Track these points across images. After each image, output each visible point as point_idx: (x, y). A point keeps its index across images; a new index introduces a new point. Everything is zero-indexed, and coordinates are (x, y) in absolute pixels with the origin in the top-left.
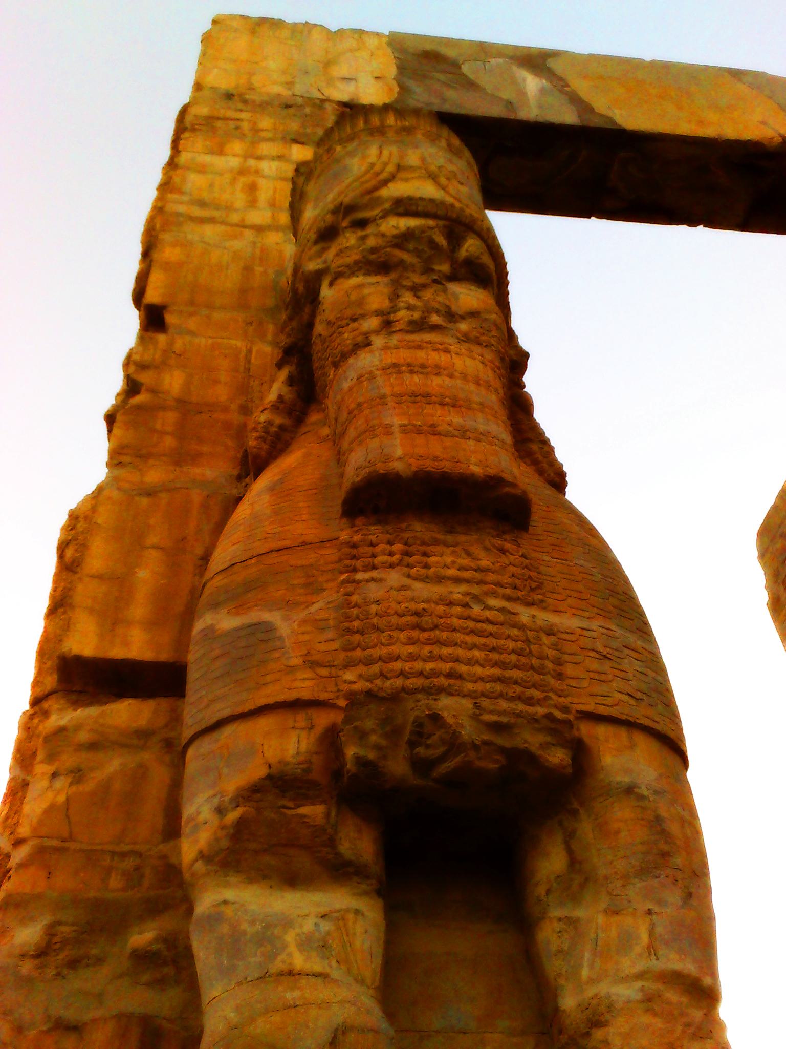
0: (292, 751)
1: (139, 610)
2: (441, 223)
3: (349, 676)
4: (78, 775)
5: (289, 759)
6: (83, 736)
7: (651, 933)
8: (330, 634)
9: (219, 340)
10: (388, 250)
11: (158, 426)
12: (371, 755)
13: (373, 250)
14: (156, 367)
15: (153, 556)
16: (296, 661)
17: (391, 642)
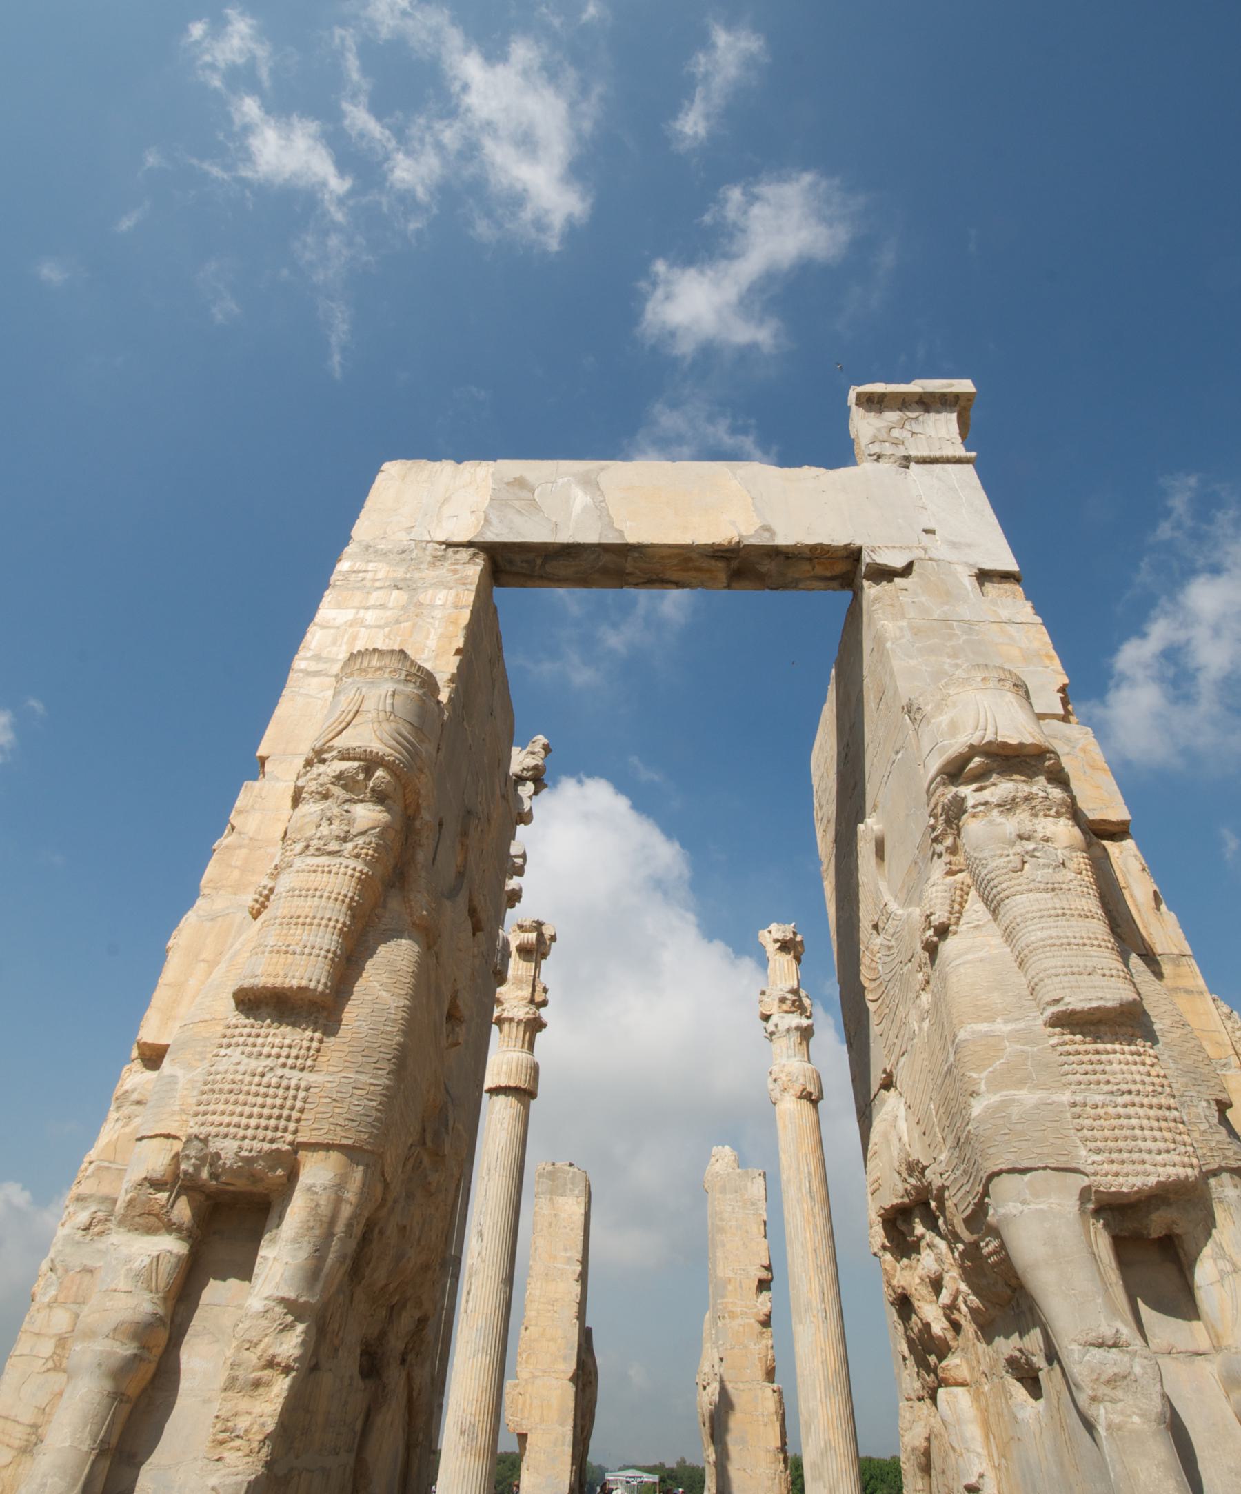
5: (157, 1168)
8: (195, 1093)
12: (191, 1170)
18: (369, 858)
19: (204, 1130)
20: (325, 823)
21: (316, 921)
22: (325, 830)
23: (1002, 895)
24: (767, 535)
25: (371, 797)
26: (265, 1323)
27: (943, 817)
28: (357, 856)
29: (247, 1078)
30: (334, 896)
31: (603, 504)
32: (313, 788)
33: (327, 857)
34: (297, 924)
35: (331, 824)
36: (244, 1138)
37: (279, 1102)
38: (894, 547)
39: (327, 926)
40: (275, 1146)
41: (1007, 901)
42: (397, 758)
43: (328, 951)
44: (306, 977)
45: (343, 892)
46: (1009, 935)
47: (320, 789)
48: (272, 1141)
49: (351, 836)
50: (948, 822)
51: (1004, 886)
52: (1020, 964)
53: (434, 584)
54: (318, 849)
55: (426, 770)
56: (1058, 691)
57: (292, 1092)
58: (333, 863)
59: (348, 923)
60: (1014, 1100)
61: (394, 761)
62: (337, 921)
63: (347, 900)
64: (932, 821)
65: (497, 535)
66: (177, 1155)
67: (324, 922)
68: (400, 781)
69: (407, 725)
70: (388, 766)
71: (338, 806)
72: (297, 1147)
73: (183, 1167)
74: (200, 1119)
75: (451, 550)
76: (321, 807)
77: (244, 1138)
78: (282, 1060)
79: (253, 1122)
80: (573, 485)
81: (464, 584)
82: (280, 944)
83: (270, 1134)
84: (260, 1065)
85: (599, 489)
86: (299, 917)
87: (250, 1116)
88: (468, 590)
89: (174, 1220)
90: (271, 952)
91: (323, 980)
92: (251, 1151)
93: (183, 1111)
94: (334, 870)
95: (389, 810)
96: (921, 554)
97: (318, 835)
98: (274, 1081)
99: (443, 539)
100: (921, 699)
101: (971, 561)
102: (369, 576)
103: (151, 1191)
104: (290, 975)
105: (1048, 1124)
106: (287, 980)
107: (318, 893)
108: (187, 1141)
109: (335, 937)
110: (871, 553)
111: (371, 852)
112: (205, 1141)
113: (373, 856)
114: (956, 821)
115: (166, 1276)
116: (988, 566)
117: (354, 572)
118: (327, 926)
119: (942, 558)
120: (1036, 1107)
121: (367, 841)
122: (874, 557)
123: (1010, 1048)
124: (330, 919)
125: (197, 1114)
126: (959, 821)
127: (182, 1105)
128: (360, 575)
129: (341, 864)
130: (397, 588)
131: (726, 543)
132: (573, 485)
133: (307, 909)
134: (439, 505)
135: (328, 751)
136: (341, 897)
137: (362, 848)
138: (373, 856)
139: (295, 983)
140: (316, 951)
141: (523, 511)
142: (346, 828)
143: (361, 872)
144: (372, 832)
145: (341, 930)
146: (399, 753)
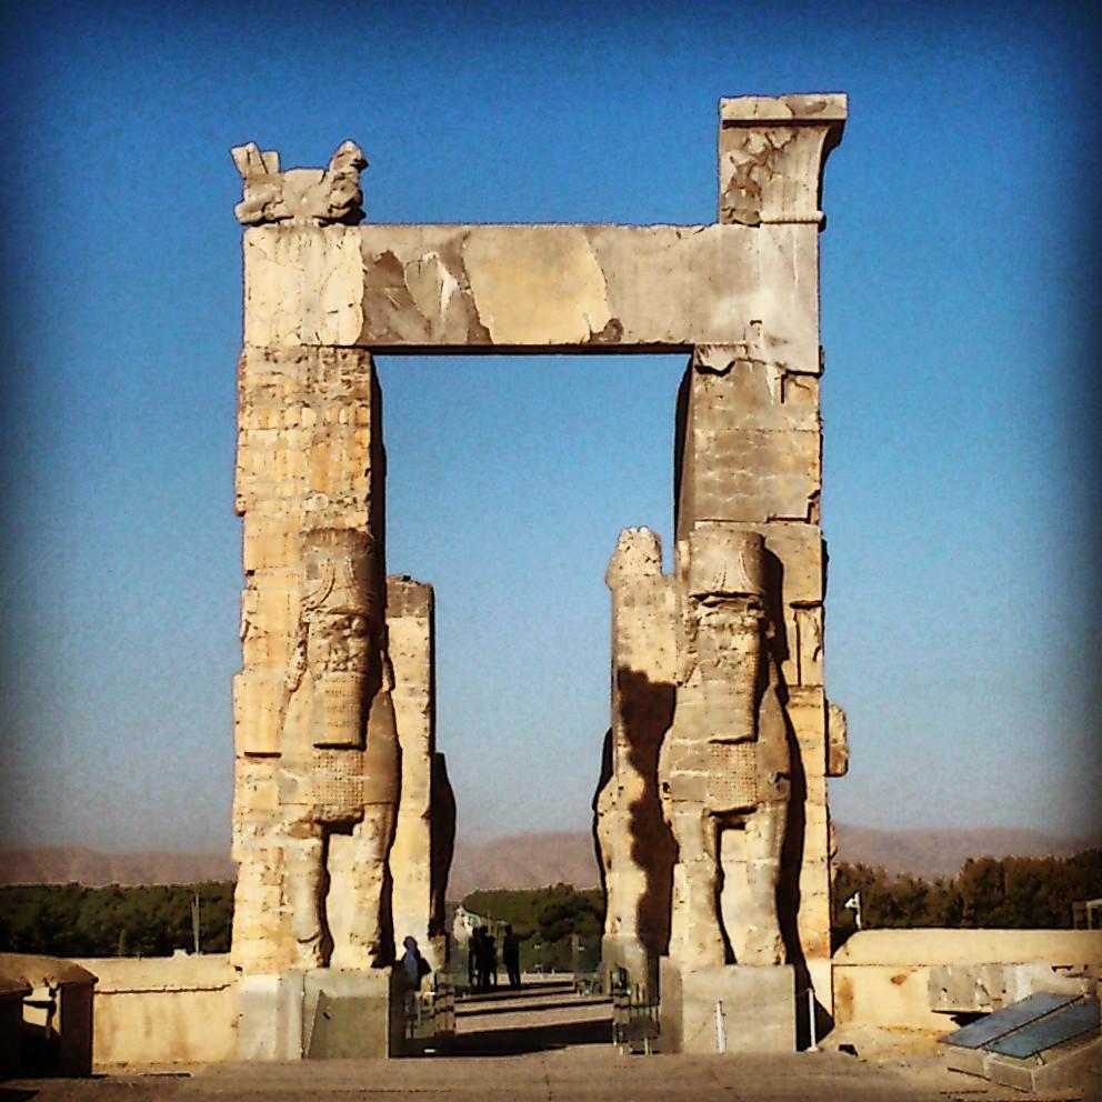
1: (264, 734)
22: (334, 657)
24: (615, 331)
31: (468, 291)
38: (721, 346)
50: (692, 625)
53: (334, 399)
65: (379, 337)
72: (363, 806)
75: (339, 351)
80: (439, 263)
81: (360, 399)
84: (339, 775)
85: (464, 271)
88: (363, 406)
96: (742, 353)
99: (331, 343)
101: (782, 362)
102: (277, 391)
110: (701, 354)
116: (792, 368)
117: (264, 387)
119: (758, 358)
122: (703, 358)
123: (689, 752)
128: (271, 390)
130: (307, 406)
131: (578, 342)
132: (439, 263)
134: (317, 294)
135: (325, 607)
141: (398, 304)
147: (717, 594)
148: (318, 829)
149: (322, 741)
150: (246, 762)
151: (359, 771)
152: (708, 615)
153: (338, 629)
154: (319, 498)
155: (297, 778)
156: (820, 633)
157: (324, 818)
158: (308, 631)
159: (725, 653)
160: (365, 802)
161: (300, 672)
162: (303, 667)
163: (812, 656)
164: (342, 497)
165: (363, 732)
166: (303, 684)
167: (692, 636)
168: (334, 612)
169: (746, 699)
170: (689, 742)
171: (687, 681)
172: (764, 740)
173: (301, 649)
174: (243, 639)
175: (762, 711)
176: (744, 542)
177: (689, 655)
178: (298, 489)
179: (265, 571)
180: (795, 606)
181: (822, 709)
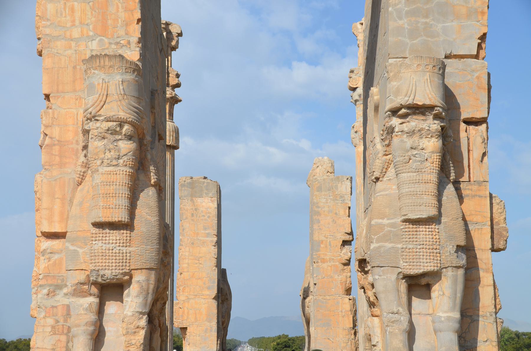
0: (82, 278)
1: (56, 218)
2: (117, 123)
3: (91, 266)
4: (49, 259)
6: (49, 251)
7: (136, 306)
8: (88, 256)
9: (68, 110)
10: (103, 134)
11: (54, 153)
12: (95, 279)
13: (101, 133)
14: (51, 126)
15: (58, 200)
16: (82, 261)
17: (98, 259)
18: (131, 165)
19: (97, 268)
20: (107, 152)
21: (117, 195)
22: (108, 155)
23: (398, 172)
25: (125, 138)
26: (134, 318)
27: (386, 132)
28: (126, 166)
29: (107, 251)
30: (121, 184)
32: (96, 134)
33: (113, 167)
34: (109, 197)
35: (110, 152)
36: (112, 270)
37: (121, 258)
39: (122, 196)
40: (124, 271)
41: (399, 175)
42: (133, 119)
43: (125, 206)
44: (120, 217)
45: (124, 182)
46: (398, 187)
47: (100, 135)
48: (122, 270)
49: (121, 157)
51: (400, 169)
52: (399, 198)
54: (109, 164)
55: (145, 117)
56: (479, 39)
57: (125, 255)
58: (117, 170)
59: (129, 194)
60: (383, 246)
61: (132, 121)
62: (125, 194)
63: (127, 185)
64: (382, 132)
66: (88, 275)
67: (120, 195)
68: (135, 128)
69: (133, 98)
70: (131, 123)
71: (111, 143)
73: (91, 279)
74: (93, 264)
76: (103, 143)
77: (112, 270)
78: (118, 244)
79: (114, 265)
82: (105, 205)
83: (121, 268)
84: (111, 246)
86: (109, 194)
87: (112, 263)
89: (92, 293)
90: (103, 208)
91: (126, 217)
92: (116, 273)
93: (85, 262)
94: (118, 173)
95: (134, 142)
97: (106, 157)
98: (117, 251)
100: (390, 68)
103: (81, 286)
104: (114, 216)
105: (392, 254)
106: (113, 218)
107: (114, 183)
108: (91, 271)
109: (126, 200)
111: (131, 163)
112: (98, 271)
113: (132, 164)
114: (391, 134)
115: (95, 308)
118: (122, 196)
120: (390, 248)
121: (128, 158)
123: (387, 229)
124: (122, 194)
125: (92, 263)
126: (392, 134)
127: (84, 260)
129: (120, 170)
133: (112, 190)
135: (100, 116)
136: (124, 184)
137: (127, 162)
138: (132, 164)
139: (117, 220)
140: (121, 207)
142: (118, 154)
143: (129, 172)
144: (129, 154)
145: (128, 197)
146: (135, 116)
147: (409, 107)
148: (94, 290)
149: (98, 220)
150: (43, 239)
151: (128, 243)
152: (401, 124)
153: (111, 134)
154: (101, 40)
155: (78, 249)
156: (485, 141)
157: (100, 280)
158: (89, 138)
159: (415, 152)
160: (132, 268)
161: (83, 170)
162: (86, 166)
163: (480, 159)
164: (118, 40)
165: (132, 214)
166: (87, 179)
167: (387, 142)
168: (108, 120)
169: (432, 188)
170: (385, 221)
171: (383, 177)
172: (445, 220)
173: (85, 152)
174: (41, 147)
175: (444, 198)
176: (430, 67)
177: (385, 157)
178: (85, 32)
179: (59, 94)
180: (469, 122)
181: (488, 199)
